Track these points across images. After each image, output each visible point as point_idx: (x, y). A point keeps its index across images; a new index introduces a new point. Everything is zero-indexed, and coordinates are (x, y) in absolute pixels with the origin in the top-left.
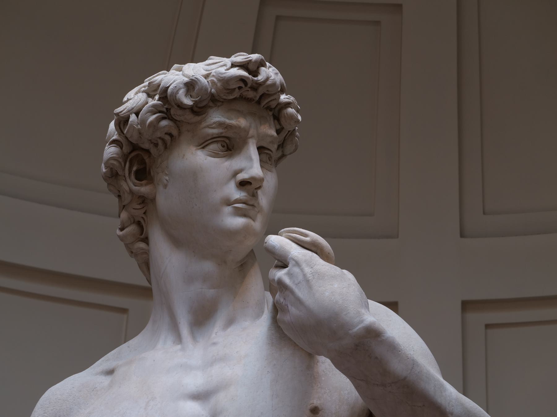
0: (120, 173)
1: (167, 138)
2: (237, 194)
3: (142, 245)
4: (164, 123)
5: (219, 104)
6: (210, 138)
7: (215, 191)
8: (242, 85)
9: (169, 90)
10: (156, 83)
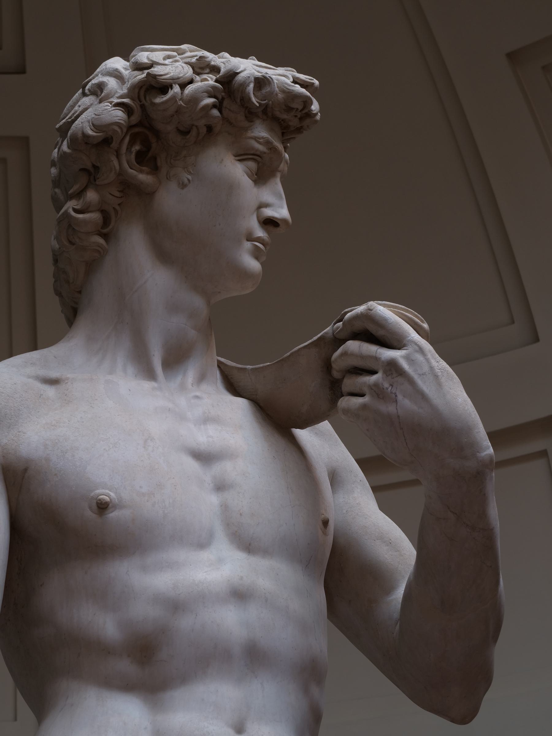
0: (114, 145)
1: (204, 130)
2: (260, 233)
3: (101, 241)
4: (215, 112)
6: (252, 152)
7: (244, 217)
8: (300, 108)
9: (240, 77)
10: (208, 60)
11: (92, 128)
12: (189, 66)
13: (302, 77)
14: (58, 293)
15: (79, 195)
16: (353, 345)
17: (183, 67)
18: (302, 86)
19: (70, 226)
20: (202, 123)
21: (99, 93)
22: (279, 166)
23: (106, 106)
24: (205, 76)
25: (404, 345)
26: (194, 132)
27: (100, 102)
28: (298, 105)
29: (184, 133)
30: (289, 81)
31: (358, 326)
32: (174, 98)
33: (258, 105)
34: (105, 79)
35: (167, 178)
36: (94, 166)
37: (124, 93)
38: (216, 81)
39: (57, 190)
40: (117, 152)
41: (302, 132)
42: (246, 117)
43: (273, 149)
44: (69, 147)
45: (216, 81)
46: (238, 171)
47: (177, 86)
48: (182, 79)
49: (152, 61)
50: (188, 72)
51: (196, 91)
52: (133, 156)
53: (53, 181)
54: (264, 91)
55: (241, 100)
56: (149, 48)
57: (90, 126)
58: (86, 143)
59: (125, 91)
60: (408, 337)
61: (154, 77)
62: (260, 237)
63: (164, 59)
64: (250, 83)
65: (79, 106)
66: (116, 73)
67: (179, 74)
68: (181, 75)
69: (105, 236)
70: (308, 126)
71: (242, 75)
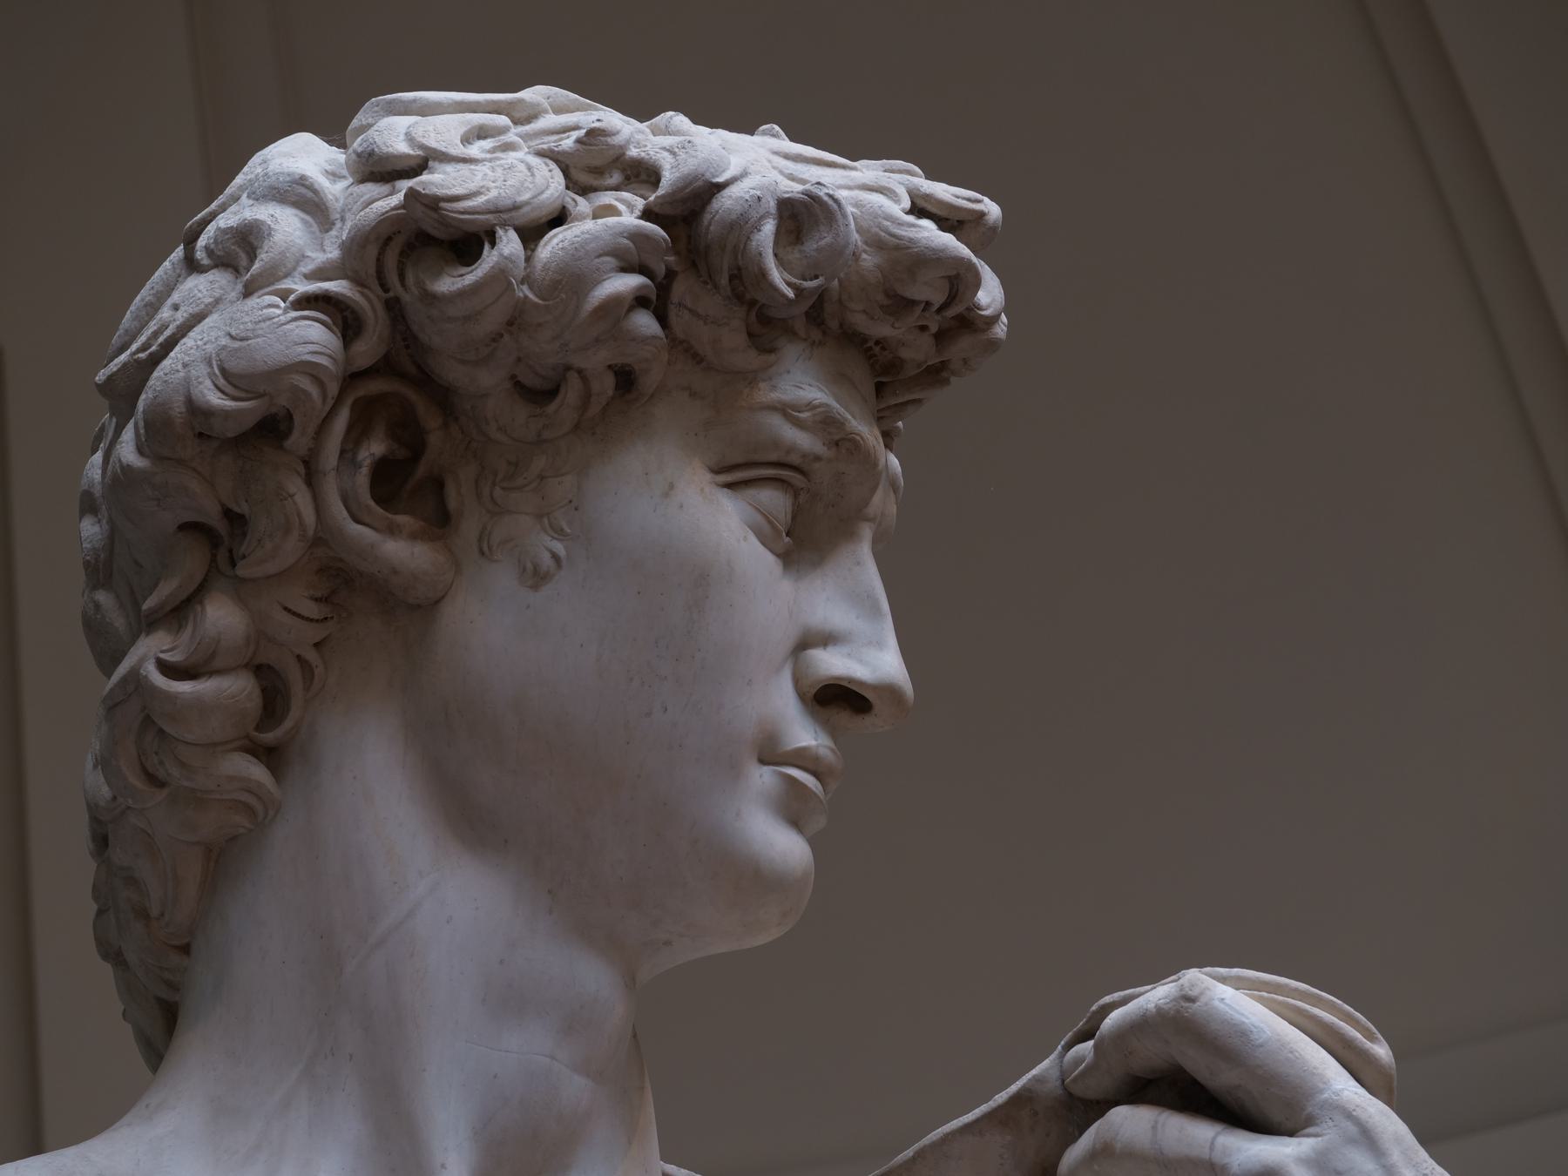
0: (298, 441)
2: (804, 734)
3: (257, 772)
4: (645, 322)
5: (816, 334)
6: (773, 457)
7: (750, 682)
8: (938, 298)
9: (726, 202)
10: (616, 140)
11: (221, 382)
12: (553, 166)
13: (944, 191)
14: (114, 956)
15: (178, 613)
16: (1131, 1123)
17: (530, 168)
18: (944, 224)
19: (148, 721)
20: (597, 360)
21: (244, 261)
22: (866, 502)
23: (267, 305)
24: (607, 198)
25: (1310, 1121)
26: (571, 393)
27: (248, 293)
28: (929, 291)
29: (540, 394)
30: (897, 209)
31: (1150, 1056)
32: (500, 276)
33: (790, 294)
34: (265, 213)
35: (482, 553)
36: (228, 513)
37: (330, 262)
38: (647, 215)
39: (102, 597)
40: (306, 463)
41: (946, 382)
42: (750, 335)
43: (844, 444)
44: (140, 450)
45: (647, 215)
46: (725, 524)
47: (513, 235)
48: (525, 209)
49: (422, 147)
50: (550, 184)
51: (577, 252)
52: (363, 479)
53: (87, 564)
54: (811, 246)
55: (732, 278)
56: (414, 101)
57: (211, 375)
58: (201, 435)
59: (333, 253)
60: (1322, 1091)
61: (433, 203)
62: (804, 749)
63: (466, 140)
64: (762, 218)
65: (176, 308)
66: (303, 190)
67: (519, 193)
68: (526, 196)
69: (271, 756)
70: (965, 361)
71: (734, 191)
